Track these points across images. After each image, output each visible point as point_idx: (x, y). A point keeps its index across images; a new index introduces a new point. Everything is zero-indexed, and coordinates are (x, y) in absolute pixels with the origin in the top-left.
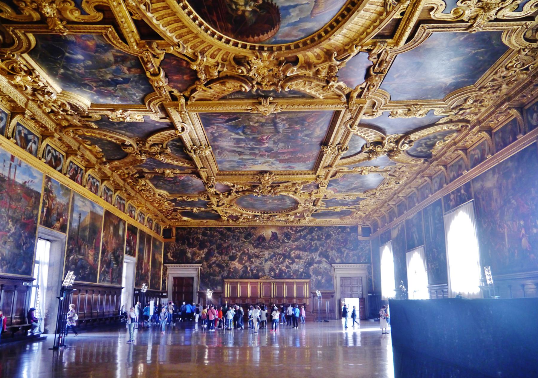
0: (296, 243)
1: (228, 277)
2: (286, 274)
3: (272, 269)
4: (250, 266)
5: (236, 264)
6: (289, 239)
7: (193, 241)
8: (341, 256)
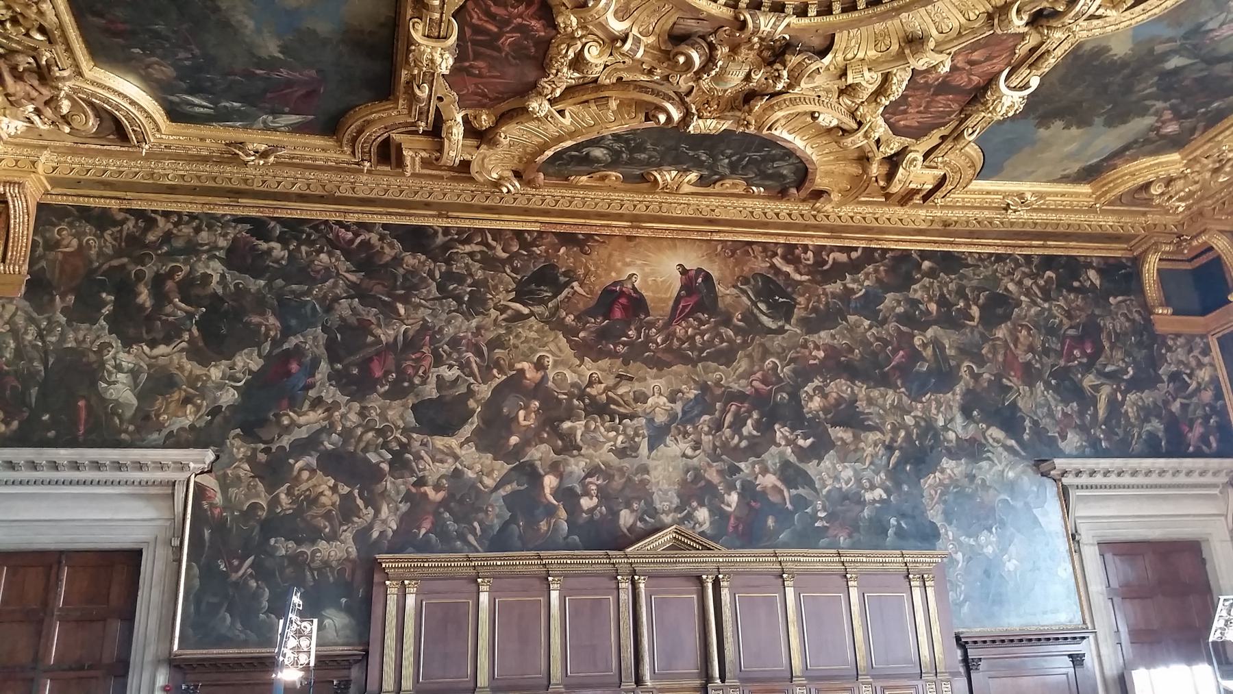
0: (824, 336)
1: (403, 541)
2: (783, 516)
3: (695, 489)
4: (554, 468)
6: (784, 311)
8: (1081, 414)
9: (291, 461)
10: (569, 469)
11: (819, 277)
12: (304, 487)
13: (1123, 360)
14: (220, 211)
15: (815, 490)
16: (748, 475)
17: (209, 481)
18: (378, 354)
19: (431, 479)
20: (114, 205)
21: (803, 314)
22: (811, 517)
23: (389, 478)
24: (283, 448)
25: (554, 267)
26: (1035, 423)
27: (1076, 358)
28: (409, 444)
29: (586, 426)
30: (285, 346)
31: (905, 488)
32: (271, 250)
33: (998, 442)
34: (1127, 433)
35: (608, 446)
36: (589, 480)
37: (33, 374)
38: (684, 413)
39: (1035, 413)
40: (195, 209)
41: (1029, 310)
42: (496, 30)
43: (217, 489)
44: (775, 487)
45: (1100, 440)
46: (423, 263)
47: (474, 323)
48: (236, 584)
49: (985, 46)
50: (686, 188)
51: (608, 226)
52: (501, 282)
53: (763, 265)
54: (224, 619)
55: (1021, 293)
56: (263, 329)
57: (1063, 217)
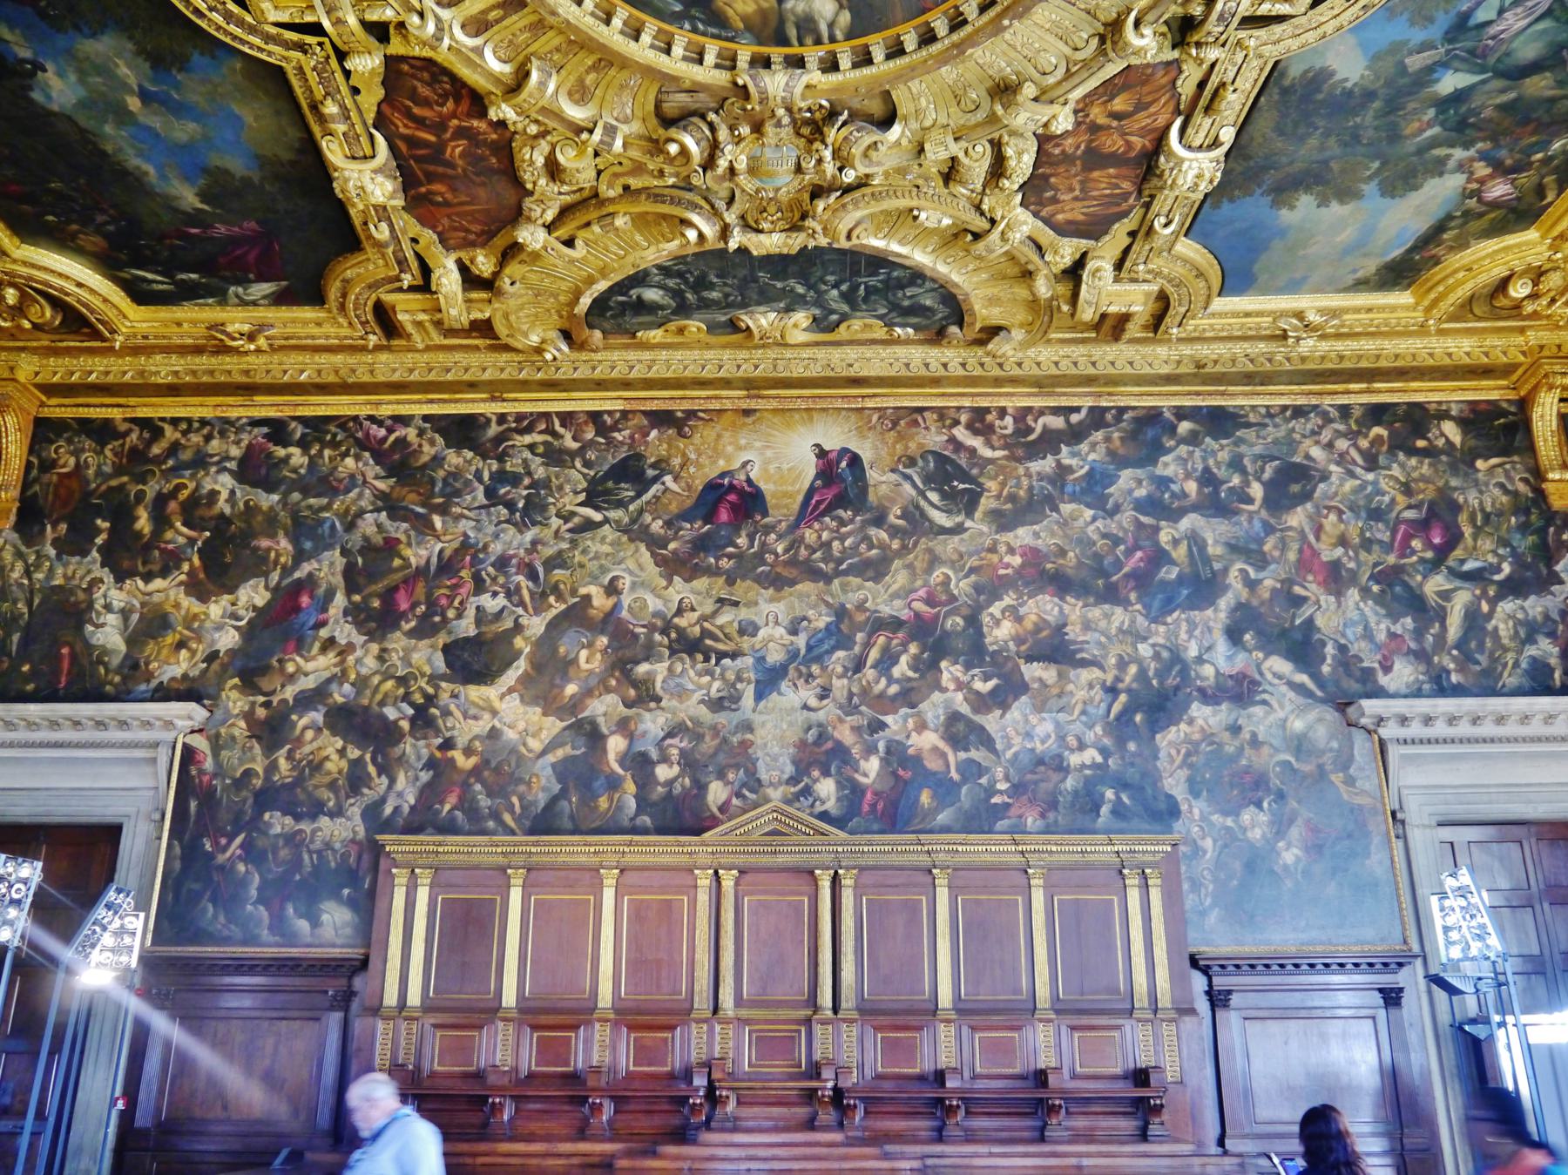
0: (1023, 535)
1: (420, 821)
2: (945, 789)
3: (820, 753)
4: (623, 726)
5: (504, 713)
7: (161, 520)
8: (1419, 634)
9: (294, 717)
10: (642, 727)
11: (1020, 452)
12: (307, 749)
13: (1494, 552)
14: (233, 414)
15: (994, 751)
16: (896, 733)
17: (200, 743)
18: (405, 581)
19: (461, 741)
20: (116, 414)
21: (993, 504)
22: (986, 790)
23: (409, 740)
24: (284, 701)
25: (639, 457)
26: (1342, 649)
27: (1414, 552)
28: (436, 696)
29: (670, 669)
30: (297, 575)
31: (1132, 746)
32: (289, 456)
33: (1280, 677)
34: (1494, 660)
35: (698, 695)
36: (669, 741)
37: (16, 618)
38: (810, 648)
39: (1344, 635)
40: (207, 413)
41: (1341, 485)
42: (432, 138)
43: (208, 752)
44: (935, 749)
45: (1448, 672)
46: (469, 462)
47: (529, 536)
48: (222, 868)
49: (1125, 87)
50: (800, 337)
51: (716, 398)
52: (568, 481)
53: (938, 439)
54: (205, 910)
55: (1330, 461)
56: (273, 554)
57: (1387, 344)
